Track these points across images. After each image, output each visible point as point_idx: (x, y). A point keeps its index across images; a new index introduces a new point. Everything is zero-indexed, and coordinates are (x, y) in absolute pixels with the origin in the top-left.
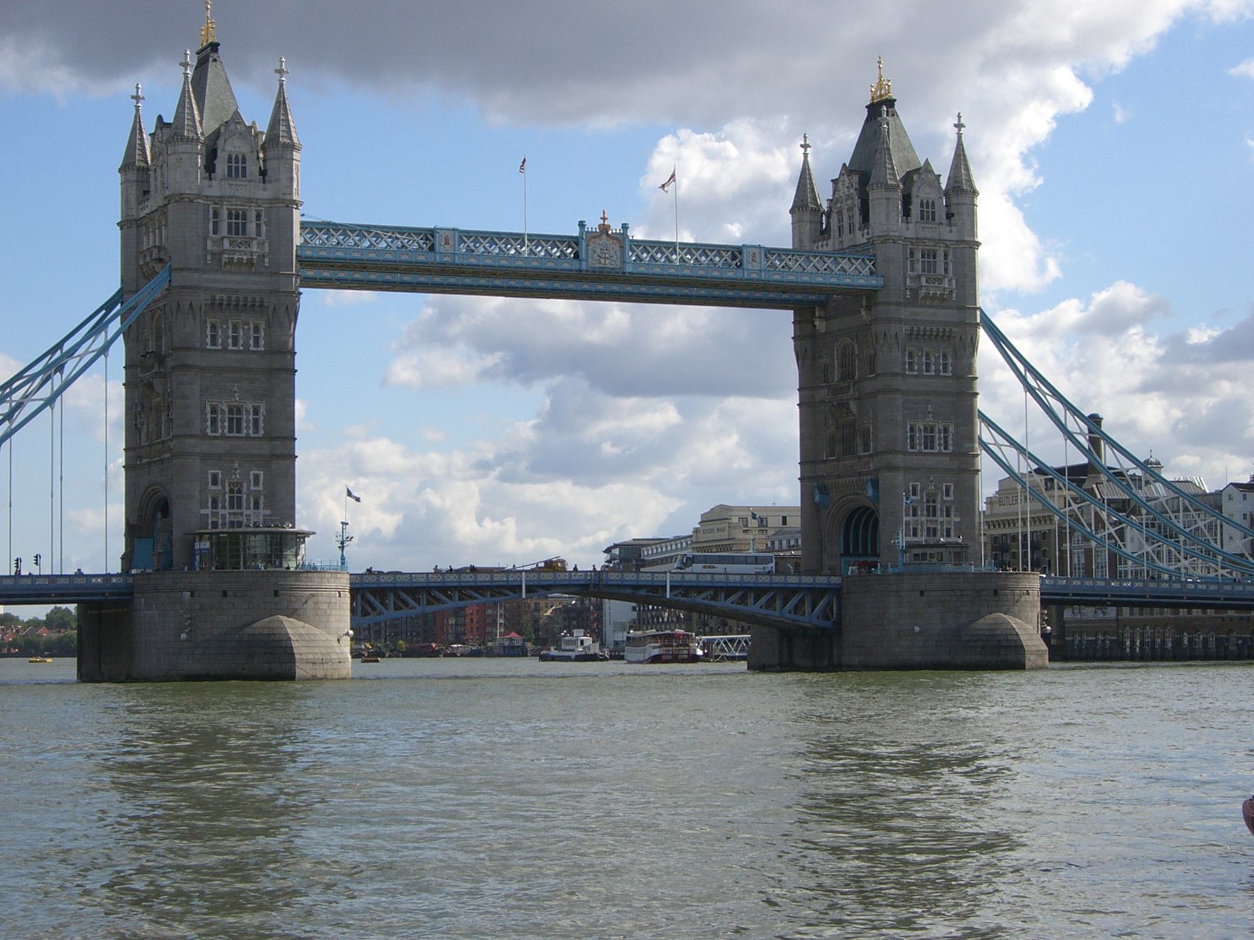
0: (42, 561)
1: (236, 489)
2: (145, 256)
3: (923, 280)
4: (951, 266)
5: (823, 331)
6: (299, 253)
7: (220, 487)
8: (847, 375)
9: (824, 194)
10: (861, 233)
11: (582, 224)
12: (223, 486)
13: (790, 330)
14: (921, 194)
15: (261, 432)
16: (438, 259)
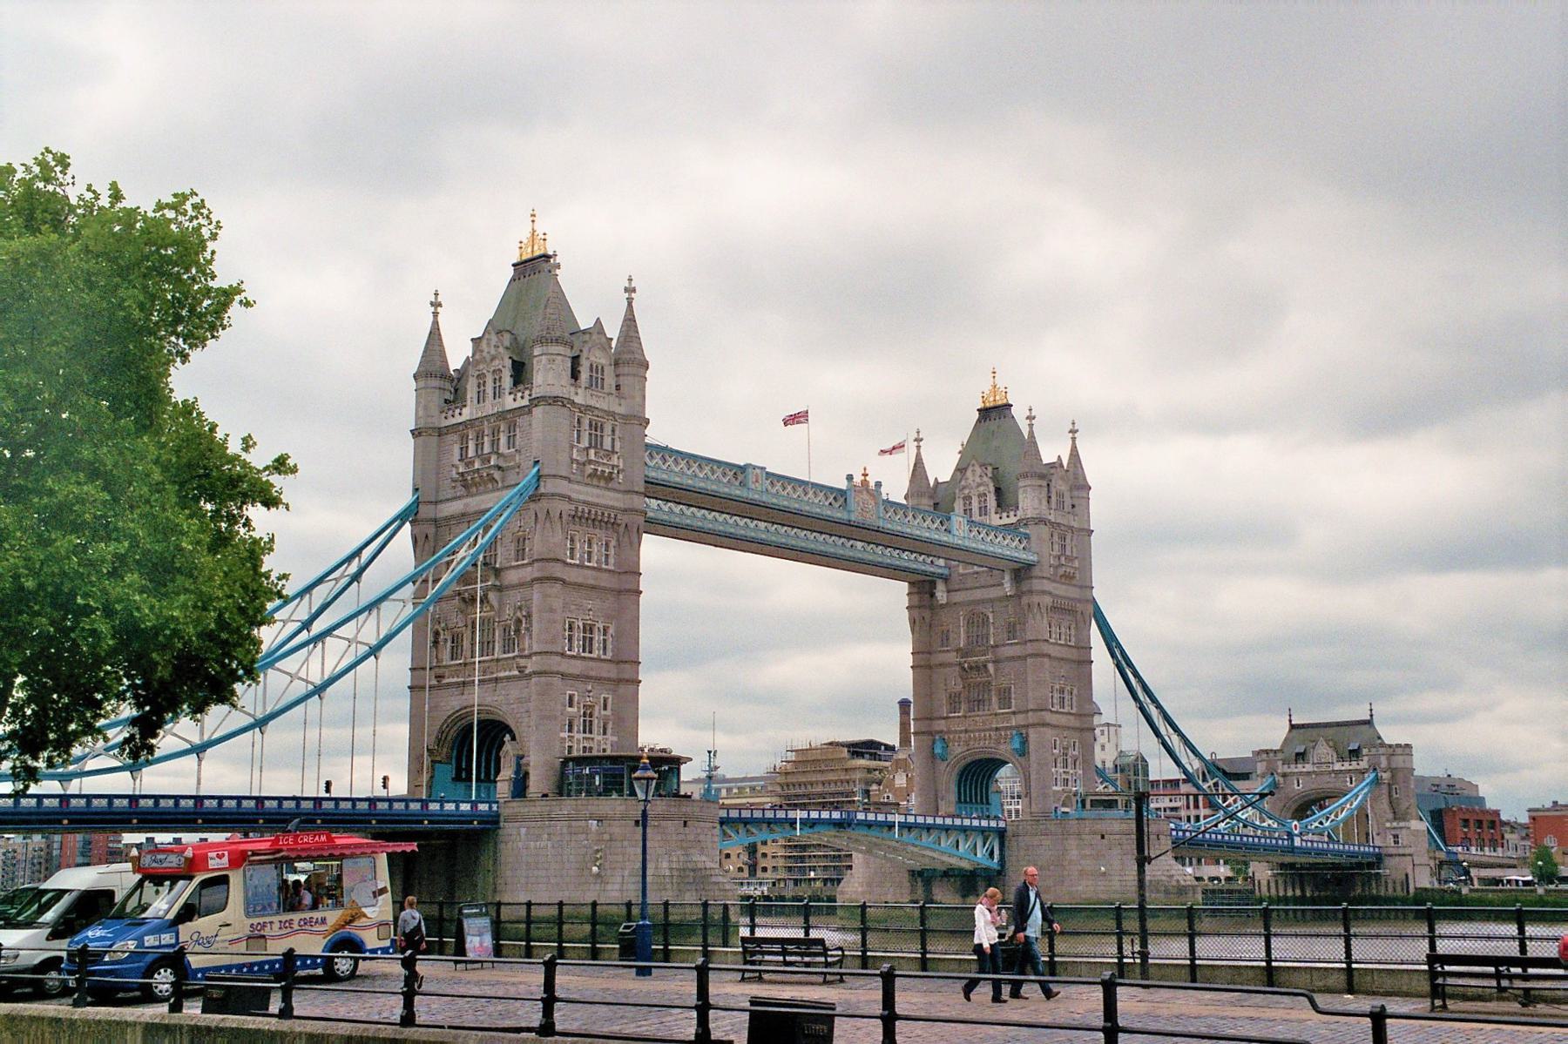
0: (391, 783)
1: (588, 714)
2: (470, 463)
3: (1063, 559)
4: (1074, 550)
5: (944, 602)
6: (646, 473)
7: (575, 709)
8: (977, 641)
9: (932, 484)
10: (998, 516)
11: (850, 478)
12: (579, 711)
13: (905, 601)
14: (1059, 485)
15: (609, 655)
16: (750, 496)
